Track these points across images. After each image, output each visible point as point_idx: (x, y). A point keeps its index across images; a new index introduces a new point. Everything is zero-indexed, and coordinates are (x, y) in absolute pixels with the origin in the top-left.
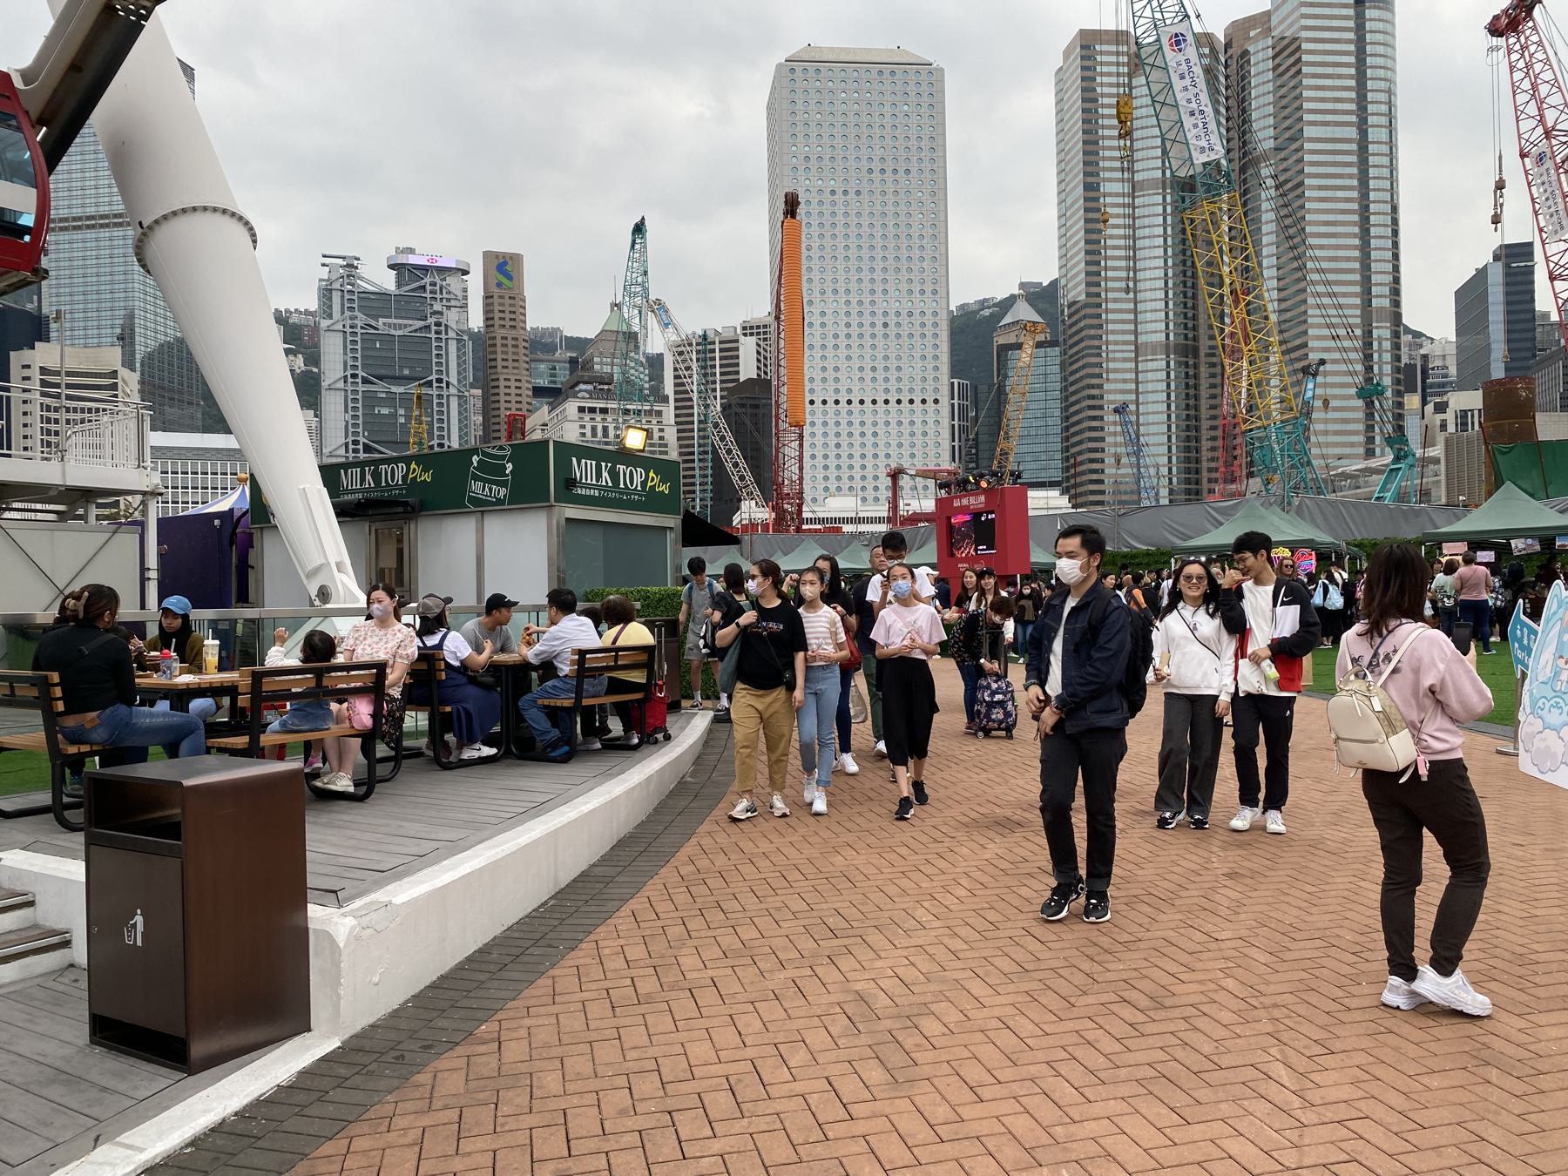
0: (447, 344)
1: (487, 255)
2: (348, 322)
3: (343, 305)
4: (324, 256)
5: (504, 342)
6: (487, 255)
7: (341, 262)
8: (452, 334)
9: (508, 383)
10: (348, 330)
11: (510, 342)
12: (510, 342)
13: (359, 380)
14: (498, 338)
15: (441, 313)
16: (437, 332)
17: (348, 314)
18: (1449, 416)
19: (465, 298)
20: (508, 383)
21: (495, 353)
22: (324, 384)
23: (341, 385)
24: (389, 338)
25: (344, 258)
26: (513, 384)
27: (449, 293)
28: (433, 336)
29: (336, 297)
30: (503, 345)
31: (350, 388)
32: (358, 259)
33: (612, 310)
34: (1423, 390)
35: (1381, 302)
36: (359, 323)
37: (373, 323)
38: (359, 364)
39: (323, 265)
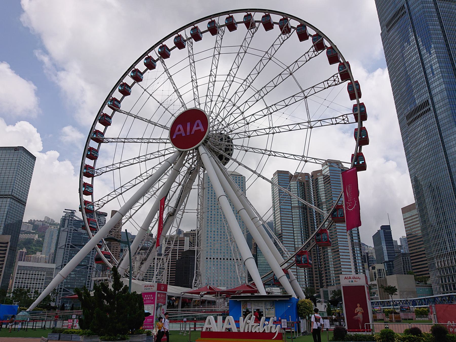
3: (68, 223)
4: (65, 210)
7: (70, 211)
9: (114, 248)
10: (69, 231)
13: (70, 246)
17: (70, 226)
18: (376, 271)
20: (114, 248)
23: (64, 247)
24: (81, 234)
25: (71, 210)
26: (115, 248)
27: (100, 221)
29: (67, 221)
31: (66, 248)
32: (75, 211)
34: (368, 262)
35: (356, 241)
36: (73, 229)
37: (77, 229)
38: (70, 241)
39: (64, 212)
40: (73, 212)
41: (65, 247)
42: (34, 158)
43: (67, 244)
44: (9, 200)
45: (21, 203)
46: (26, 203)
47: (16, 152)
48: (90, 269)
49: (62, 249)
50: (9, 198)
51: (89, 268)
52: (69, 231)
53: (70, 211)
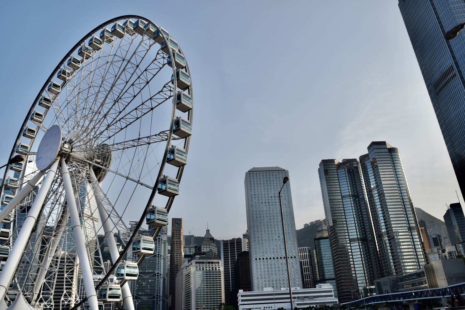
0: (161, 244)
1: (173, 219)
4: (130, 222)
5: (177, 243)
6: (173, 219)
7: (134, 223)
8: (162, 241)
9: (177, 254)
11: (178, 243)
12: (178, 243)
14: (175, 242)
15: (160, 236)
16: (159, 241)
19: (167, 231)
20: (177, 254)
21: (174, 246)
25: (135, 222)
28: (158, 242)
30: (176, 244)
33: (207, 232)
48: (158, 276)
51: (157, 275)
53: (134, 223)
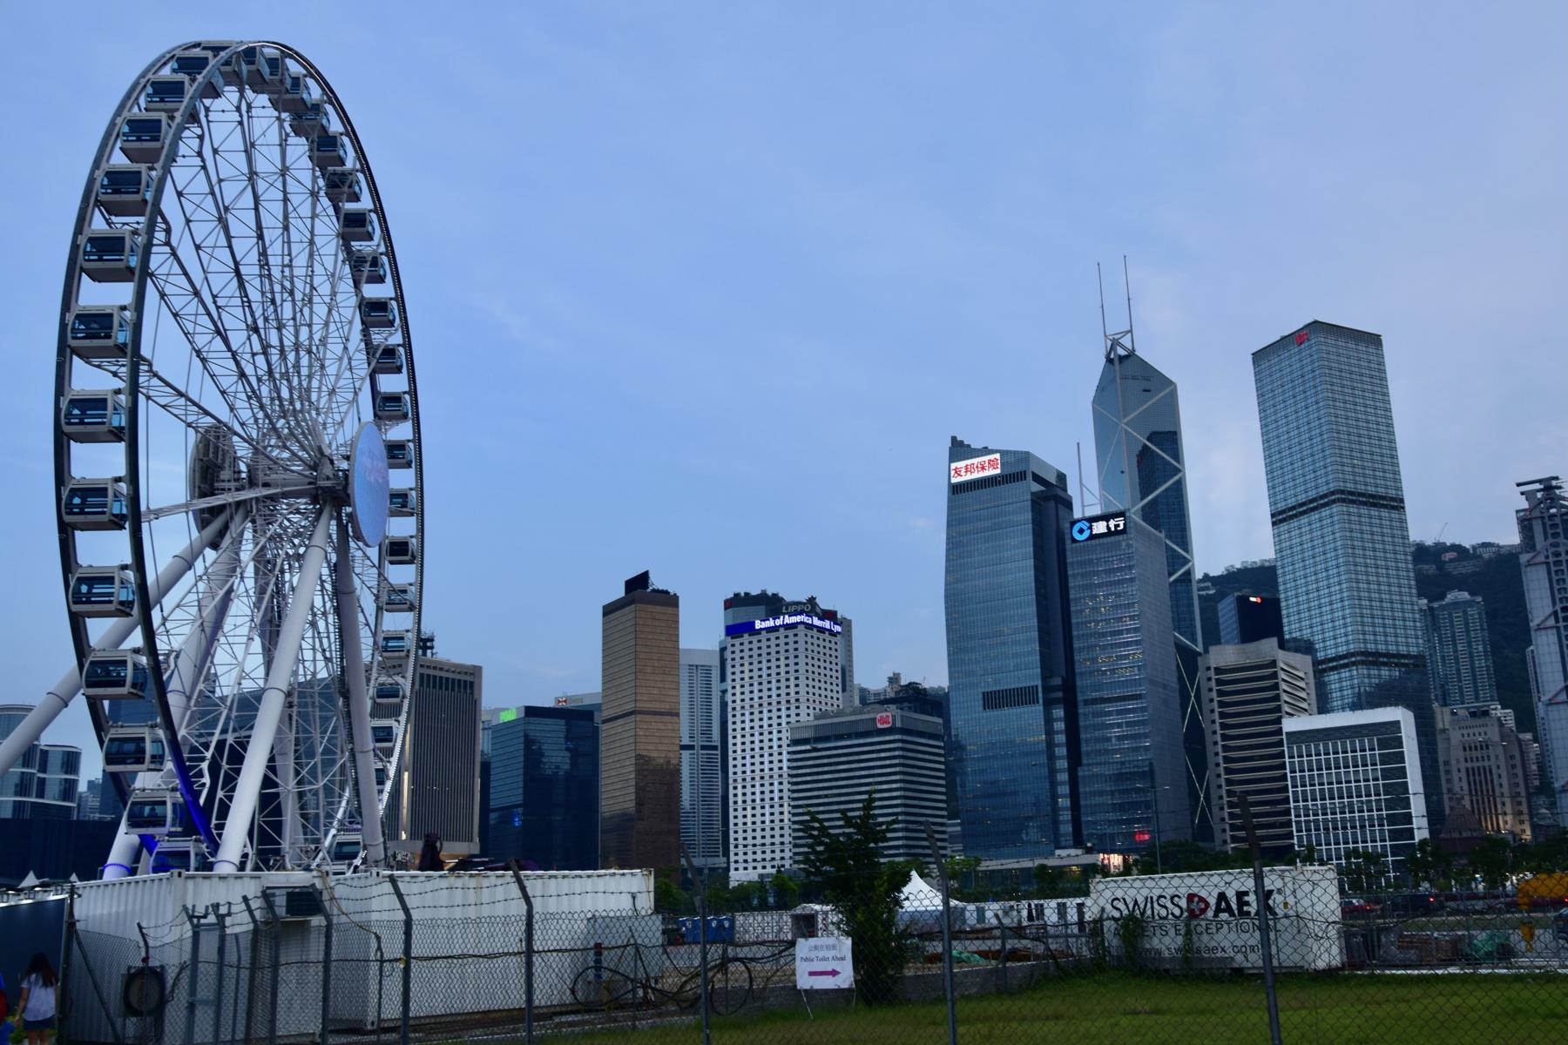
2: (1552, 550)
4: (1519, 485)
7: (1538, 486)
10: (1551, 559)
22: (1533, 625)
23: (1551, 622)
25: (1539, 481)
32: (1556, 478)
39: (1522, 493)
40: (1547, 484)
41: (1557, 621)
42: (1374, 340)
43: (1558, 607)
44: (1336, 508)
45: (1385, 506)
46: (1402, 501)
47: (1303, 346)
49: (1550, 631)
50: (1334, 501)
52: (1551, 559)
